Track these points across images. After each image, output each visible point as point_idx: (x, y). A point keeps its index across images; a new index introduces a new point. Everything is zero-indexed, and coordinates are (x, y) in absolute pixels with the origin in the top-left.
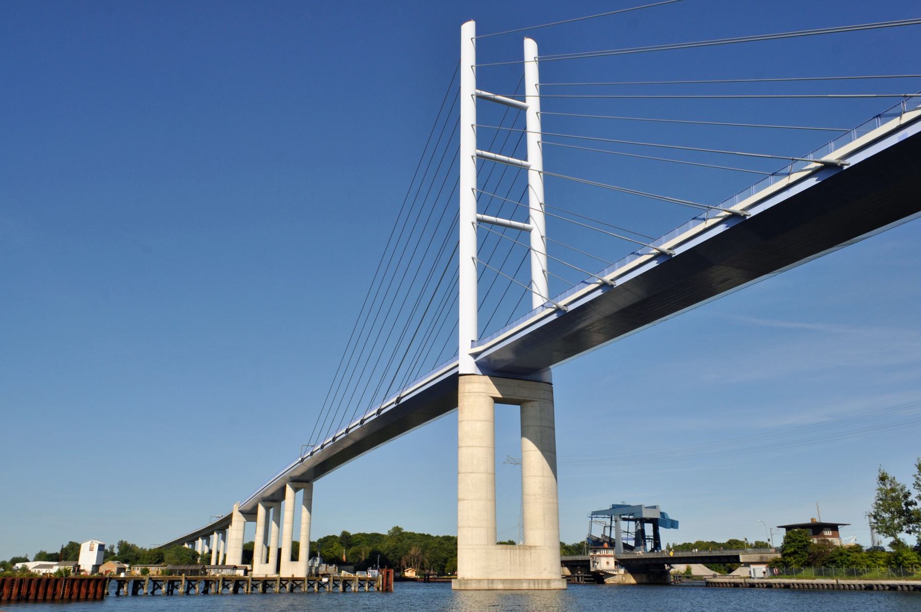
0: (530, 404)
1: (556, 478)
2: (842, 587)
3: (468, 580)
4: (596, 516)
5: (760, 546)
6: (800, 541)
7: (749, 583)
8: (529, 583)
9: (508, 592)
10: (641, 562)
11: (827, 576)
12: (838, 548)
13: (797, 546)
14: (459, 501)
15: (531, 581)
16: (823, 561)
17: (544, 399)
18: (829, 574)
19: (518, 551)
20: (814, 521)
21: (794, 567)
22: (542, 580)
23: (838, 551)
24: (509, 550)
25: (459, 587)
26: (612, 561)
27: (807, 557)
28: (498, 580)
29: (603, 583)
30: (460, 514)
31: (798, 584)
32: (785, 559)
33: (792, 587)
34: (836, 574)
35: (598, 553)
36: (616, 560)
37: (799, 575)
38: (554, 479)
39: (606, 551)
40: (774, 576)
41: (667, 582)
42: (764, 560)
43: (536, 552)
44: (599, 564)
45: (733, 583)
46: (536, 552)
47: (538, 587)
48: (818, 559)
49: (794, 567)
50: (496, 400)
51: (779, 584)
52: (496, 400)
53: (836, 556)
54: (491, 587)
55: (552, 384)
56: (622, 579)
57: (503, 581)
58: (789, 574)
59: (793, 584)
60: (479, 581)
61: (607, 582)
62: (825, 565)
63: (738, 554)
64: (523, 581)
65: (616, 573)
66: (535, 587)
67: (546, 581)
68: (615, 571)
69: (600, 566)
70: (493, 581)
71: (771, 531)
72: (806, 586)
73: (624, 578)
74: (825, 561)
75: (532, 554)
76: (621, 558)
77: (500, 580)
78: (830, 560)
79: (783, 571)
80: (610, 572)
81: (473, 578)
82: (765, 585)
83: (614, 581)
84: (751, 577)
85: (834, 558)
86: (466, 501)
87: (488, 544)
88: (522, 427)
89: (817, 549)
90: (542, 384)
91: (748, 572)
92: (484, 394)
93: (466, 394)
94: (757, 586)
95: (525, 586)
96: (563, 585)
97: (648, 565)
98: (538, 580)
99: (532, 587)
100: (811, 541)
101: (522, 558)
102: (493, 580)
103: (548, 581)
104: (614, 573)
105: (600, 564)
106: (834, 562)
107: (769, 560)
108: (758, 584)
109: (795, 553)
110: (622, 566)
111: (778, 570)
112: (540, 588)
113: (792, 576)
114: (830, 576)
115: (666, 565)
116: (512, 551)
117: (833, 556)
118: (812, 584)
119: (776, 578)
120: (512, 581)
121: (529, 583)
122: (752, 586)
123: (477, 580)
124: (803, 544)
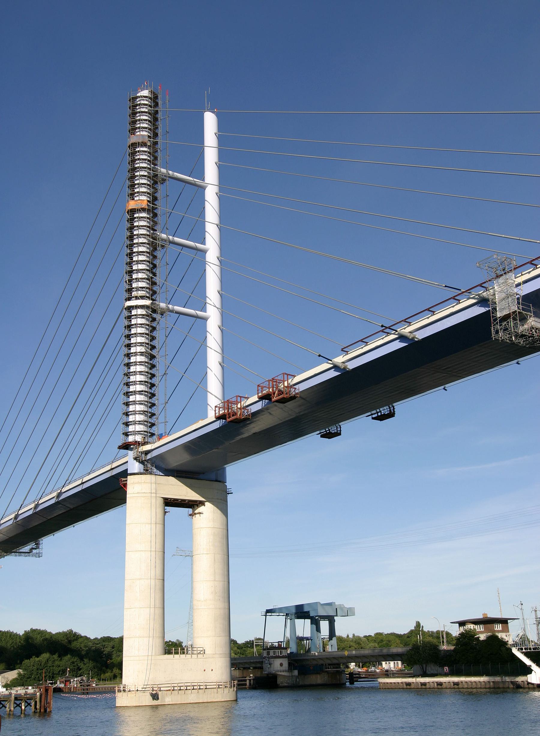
4: (270, 614)
56: (296, 680)
73: (298, 680)
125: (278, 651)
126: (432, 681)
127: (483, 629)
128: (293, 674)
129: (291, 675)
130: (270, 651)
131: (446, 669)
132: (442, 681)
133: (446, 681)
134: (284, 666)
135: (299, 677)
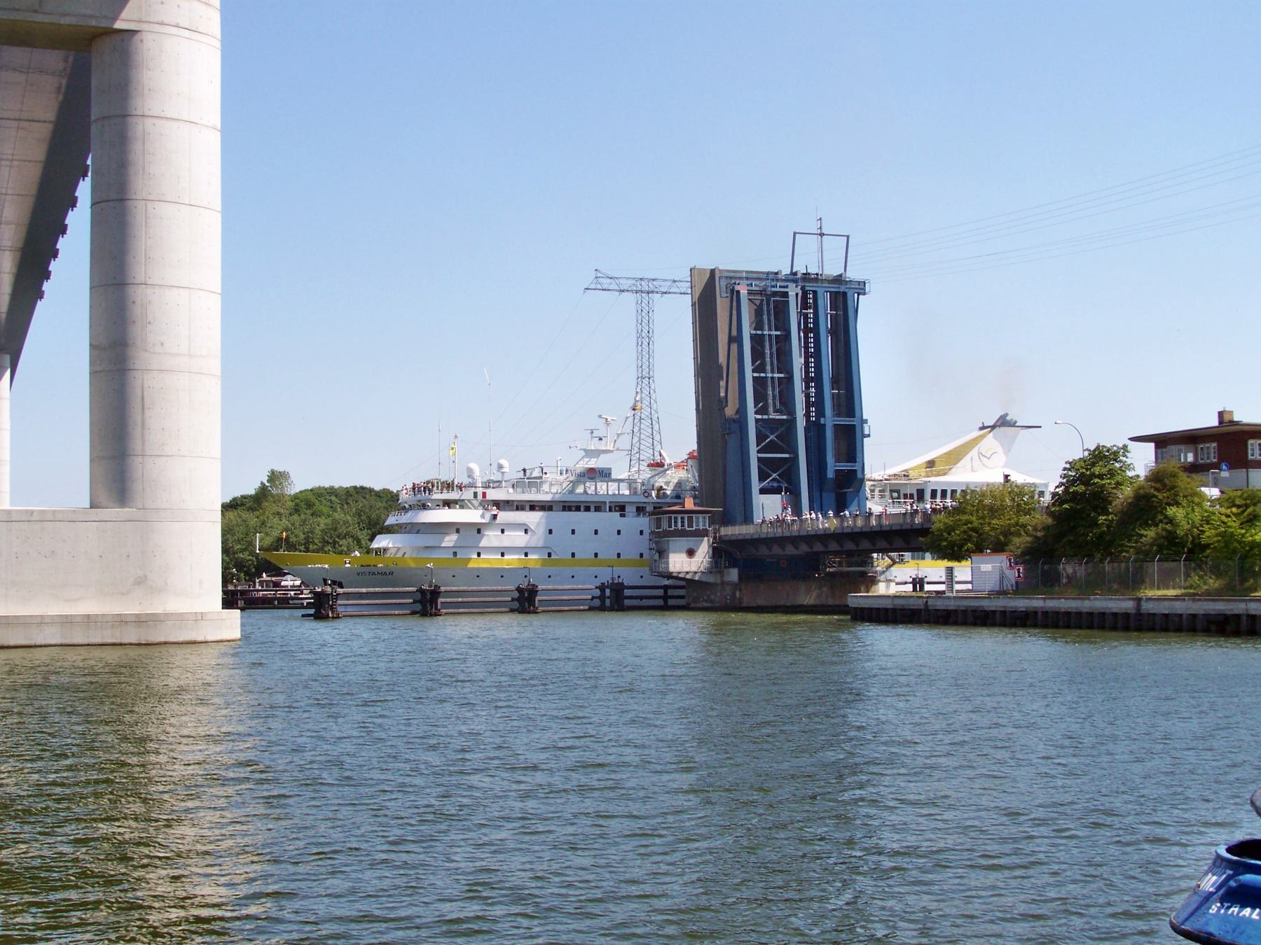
56: (734, 595)
73: (738, 595)
125: (682, 518)
127: (1214, 458)
128: (726, 579)
129: (719, 582)
132: (989, 607)
133: (996, 607)
135: (743, 587)
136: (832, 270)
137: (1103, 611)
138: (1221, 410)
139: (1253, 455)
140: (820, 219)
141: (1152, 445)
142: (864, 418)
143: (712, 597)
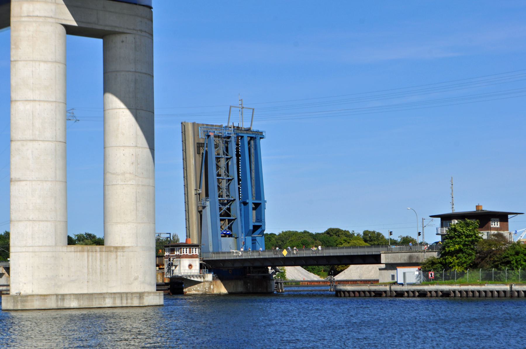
0: (118, 39)
1: (152, 149)
2: (516, 294)
3: (27, 296)
5: (406, 241)
6: (467, 236)
7: (396, 291)
8: (114, 299)
9: (85, 312)
10: (237, 265)
11: (498, 281)
12: (514, 244)
13: (462, 243)
14: (12, 183)
15: (117, 296)
16: (495, 261)
17: (141, 31)
18: (499, 277)
19: (98, 254)
20: (480, 209)
21: (457, 269)
22: (132, 294)
23: (514, 248)
24: (86, 254)
25: (14, 306)
26: (196, 263)
27: (474, 257)
28: (70, 295)
29: (182, 293)
30: (13, 200)
31: (460, 292)
32: (445, 259)
33: (452, 295)
34: (508, 278)
35: (177, 253)
36: (202, 262)
37: (460, 279)
38: (147, 151)
39: (188, 250)
40: (428, 281)
41: (269, 290)
42: (414, 261)
43: (123, 256)
44: (178, 268)
45: (374, 292)
46: (123, 256)
47: (127, 303)
48: (488, 259)
49: (457, 269)
50: (70, 30)
51: (436, 292)
52: (70, 30)
53: (511, 255)
54: (60, 305)
55: (151, 8)
56: (210, 288)
57: (78, 296)
58: (449, 279)
59: (454, 292)
60: (44, 297)
61: (188, 293)
62: (496, 267)
63: (378, 253)
64: (107, 296)
65: (202, 280)
66: (122, 303)
67: (138, 295)
68: (200, 277)
69: (180, 270)
70: (63, 297)
71: (423, 222)
72: (471, 294)
73: (212, 287)
74: (497, 261)
75: (119, 257)
76: (210, 259)
77: (74, 294)
78: (503, 260)
79: (441, 275)
80: (192, 279)
81: (34, 293)
82: (417, 294)
83: (198, 291)
84: (395, 283)
85: (508, 257)
86: (23, 183)
87: (56, 245)
88: (105, 73)
89: (488, 247)
90: (138, 6)
91: (391, 276)
92: (50, 20)
93: (24, 19)
94: (429, 294)
95: (108, 302)
96: (158, 299)
97: (245, 268)
98: (127, 293)
99: (118, 303)
100: (480, 235)
101: (104, 263)
102: (63, 295)
103: (141, 295)
104: (199, 280)
105: (180, 267)
106: (508, 263)
107: (424, 261)
108: (407, 292)
109: (460, 251)
110: (210, 272)
111: (435, 274)
112: (129, 305)
113: (452, 281)
114: (501, 281)
115: (270, 268)
116: (90, 254)
117: (507, 256)
118: (479, 292)
119: (432, 284)
120: (90, 296)
121: (114, 299)
122: (400, 294)
123: (41, 295)
124: (470, 239)
126: (413, 289)
128: (206, 279)
130: (175, 248)
131: (431, 274)
132: (427, 289)
134: (193, 268)
136: (246, 125)
137: (492, 290)
138: (477, 205)
139: (492, 225)
140: (241, 100)
141: (439, 219)
142: (265, 200)
143: (198, 288)
